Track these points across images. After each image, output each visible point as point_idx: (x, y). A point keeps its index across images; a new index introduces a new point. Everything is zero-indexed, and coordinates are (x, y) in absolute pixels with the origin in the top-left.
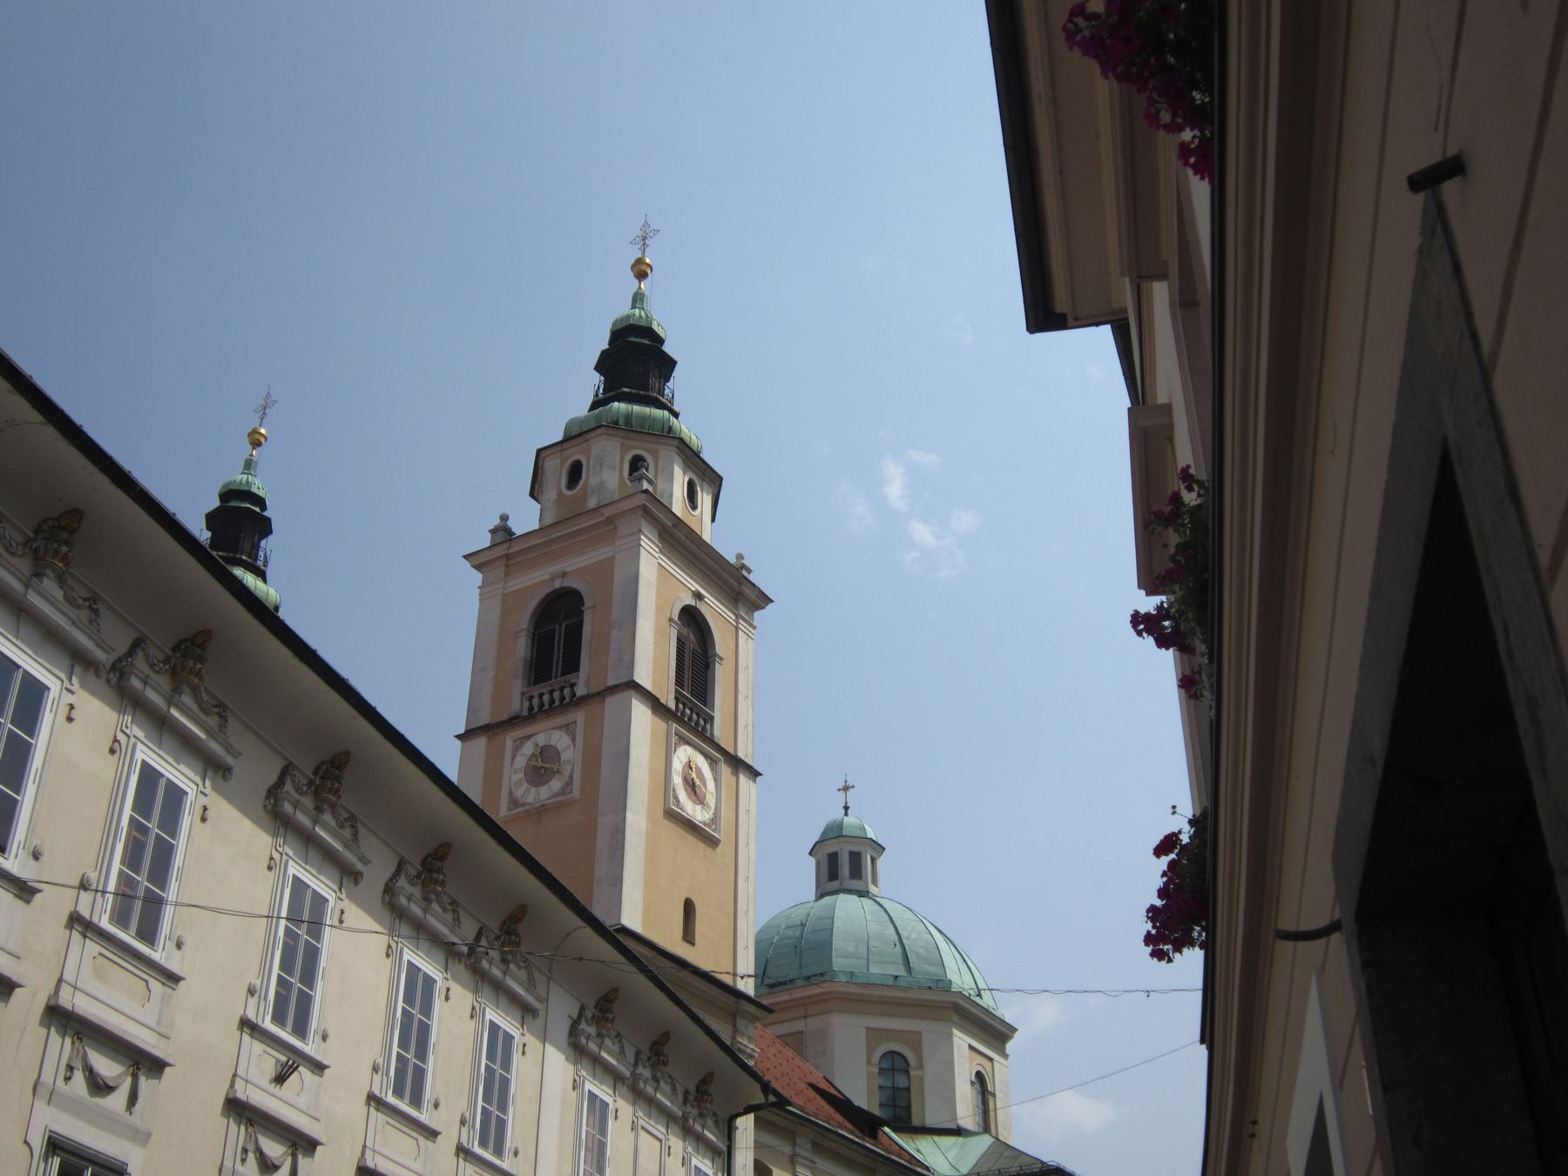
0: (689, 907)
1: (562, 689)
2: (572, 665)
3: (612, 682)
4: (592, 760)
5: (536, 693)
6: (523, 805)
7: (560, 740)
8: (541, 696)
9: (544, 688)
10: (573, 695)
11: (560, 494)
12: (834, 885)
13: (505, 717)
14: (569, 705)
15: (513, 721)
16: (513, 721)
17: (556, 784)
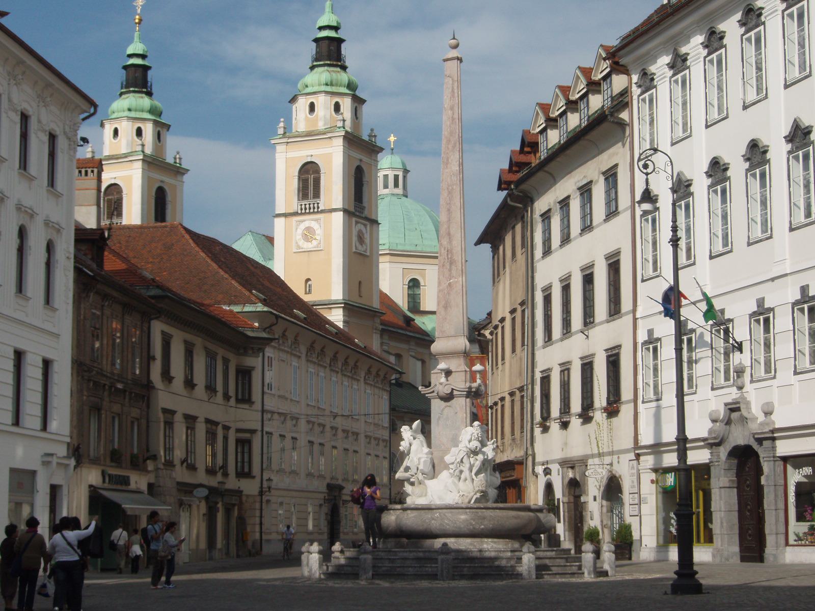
0: (360, 283)
1: (314, 204)
2: (317, 195)
3: (334, 207)
4: (328, 236)
5: (303, 203)
6: (302, 248)
7: (314, 225)
8: (305, 205)
9: (306, 202)
10: (318, 208)
11: (306, 116)
12: (386, 191)
13: (292, 211)
14: (318, 212)
15: (295, 214)
16: (295, 214)
17: (315, 243)
